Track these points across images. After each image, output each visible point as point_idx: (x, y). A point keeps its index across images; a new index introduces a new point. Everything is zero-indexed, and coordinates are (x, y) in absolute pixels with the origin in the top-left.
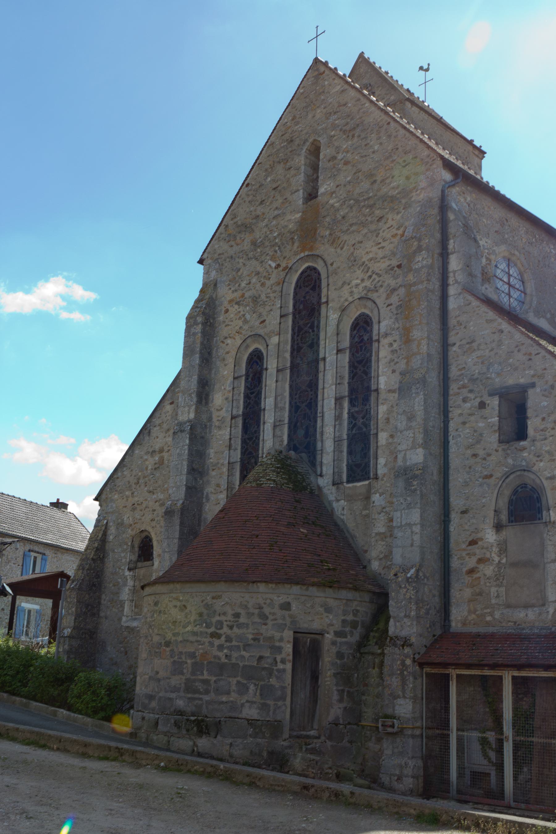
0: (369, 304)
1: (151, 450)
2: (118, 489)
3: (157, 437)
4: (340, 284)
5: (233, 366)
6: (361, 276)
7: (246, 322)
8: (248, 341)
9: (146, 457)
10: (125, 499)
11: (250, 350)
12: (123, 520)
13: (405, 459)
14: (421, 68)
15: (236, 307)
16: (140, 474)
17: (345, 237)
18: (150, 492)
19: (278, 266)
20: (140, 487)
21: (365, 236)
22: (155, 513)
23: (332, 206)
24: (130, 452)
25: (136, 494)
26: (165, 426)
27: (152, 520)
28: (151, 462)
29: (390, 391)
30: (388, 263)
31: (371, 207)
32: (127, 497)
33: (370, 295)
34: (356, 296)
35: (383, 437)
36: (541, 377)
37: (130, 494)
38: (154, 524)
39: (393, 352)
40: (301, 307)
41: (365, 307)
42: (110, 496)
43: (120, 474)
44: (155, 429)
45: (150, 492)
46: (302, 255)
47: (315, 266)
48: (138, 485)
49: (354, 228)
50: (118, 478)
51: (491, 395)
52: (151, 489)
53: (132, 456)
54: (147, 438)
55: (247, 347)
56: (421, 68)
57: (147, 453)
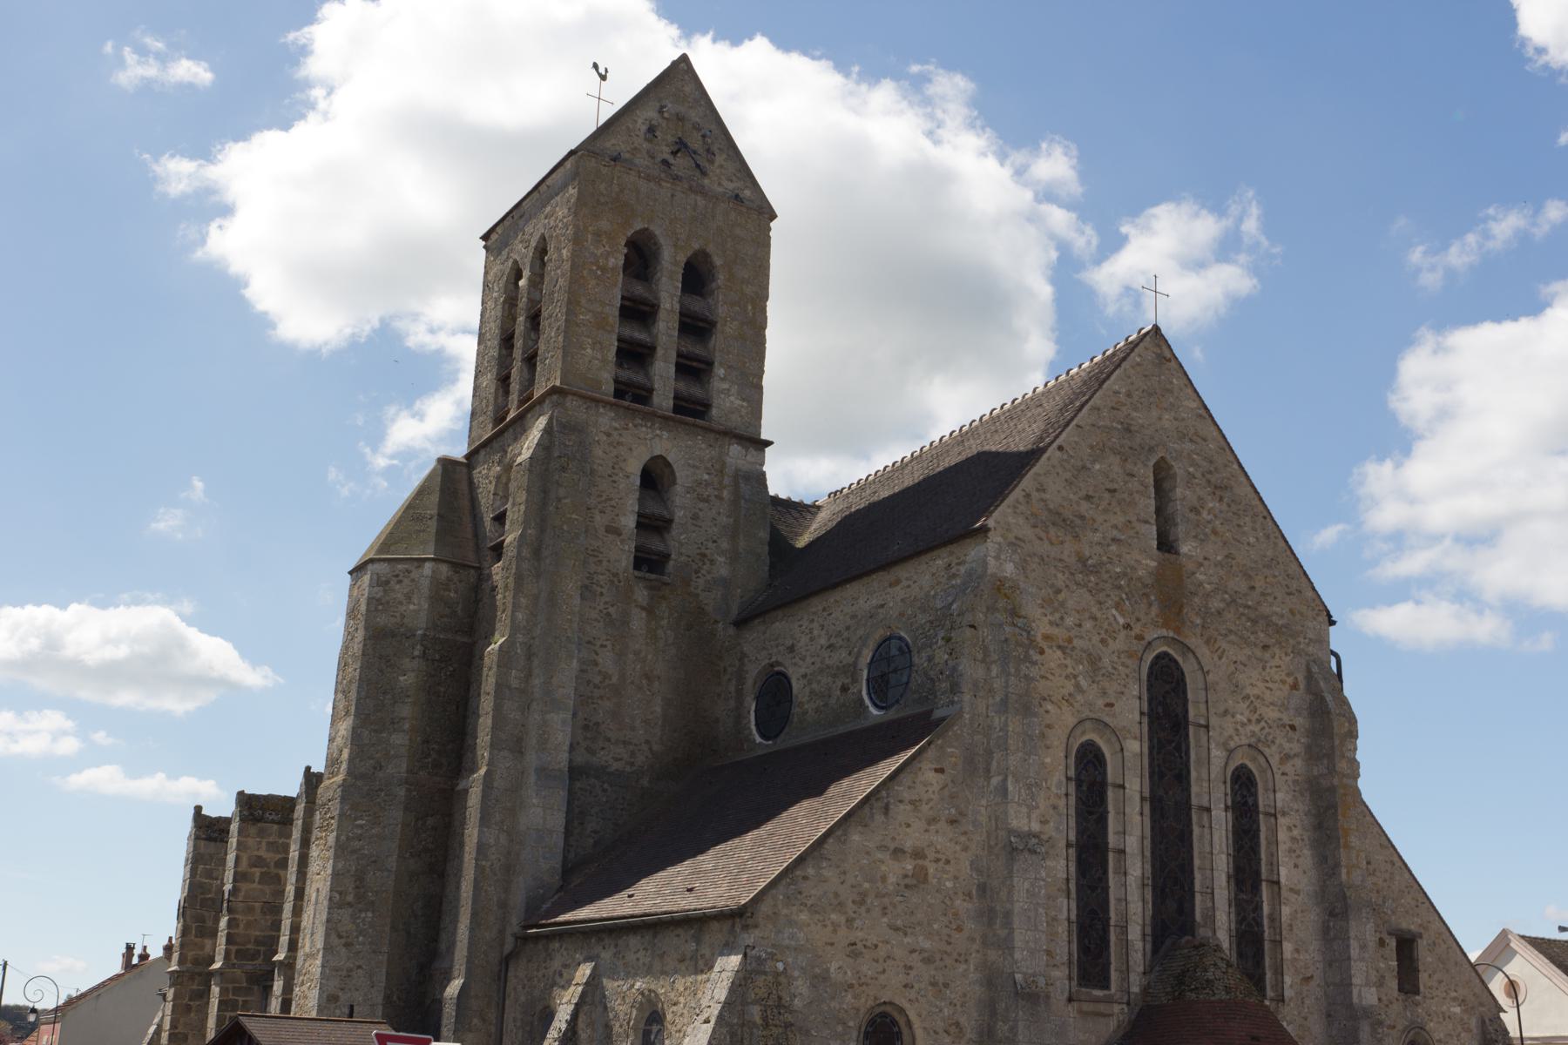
0: (1262, 760)
1: (892, 846)
2: (809, 903)
3: (909, 826)
4: (1222, 709)
5: (1062, 755)
6: (1247, 713)
7: (1078, 686)
8: (1088, 725)
9: (879, 855)
10: (830, 928)
11: (1084, 739)
12: (827, 970)
13: (1360, 995)
14: (595, 66)
15: (1059, 653)
16: (866, 885)
17: (1224, 645)
18: (897, 929)
19: (1127, 627)
20: (868, 911)
21: (1249, 657)
22: (913, 973)
23: (1201, 584)
24: (839, 833)
25: (858, 923)
26: (925, 808)
27: (905, 986)
28: (894, 871)
29: (1291, 890)
30: (1276, 715)
31: (1254, 622)
32: (836, 926)
33: (1260, 746)
34: (1245, 741)
35: (1288, 947)
36: (1426, 929)
37: (843, 919)
38: (912, 994)
39: (1293, 839)
40: (1160, 709)
41: (1254, 759)
42: (785, 911)
43: (811, 871)
44: (902, 807)
45: (897, 929)
46: (1164, 632)
47: (1180, 660)
48: (863, 909)
49: (1232, 637)
50: (805, 878)
51: (1390, 934)
52: (899, 923)
53: (844, 843)
54: (879, 818)
55: (1083, 733)
56: (595, 66)
57: (882, 848)
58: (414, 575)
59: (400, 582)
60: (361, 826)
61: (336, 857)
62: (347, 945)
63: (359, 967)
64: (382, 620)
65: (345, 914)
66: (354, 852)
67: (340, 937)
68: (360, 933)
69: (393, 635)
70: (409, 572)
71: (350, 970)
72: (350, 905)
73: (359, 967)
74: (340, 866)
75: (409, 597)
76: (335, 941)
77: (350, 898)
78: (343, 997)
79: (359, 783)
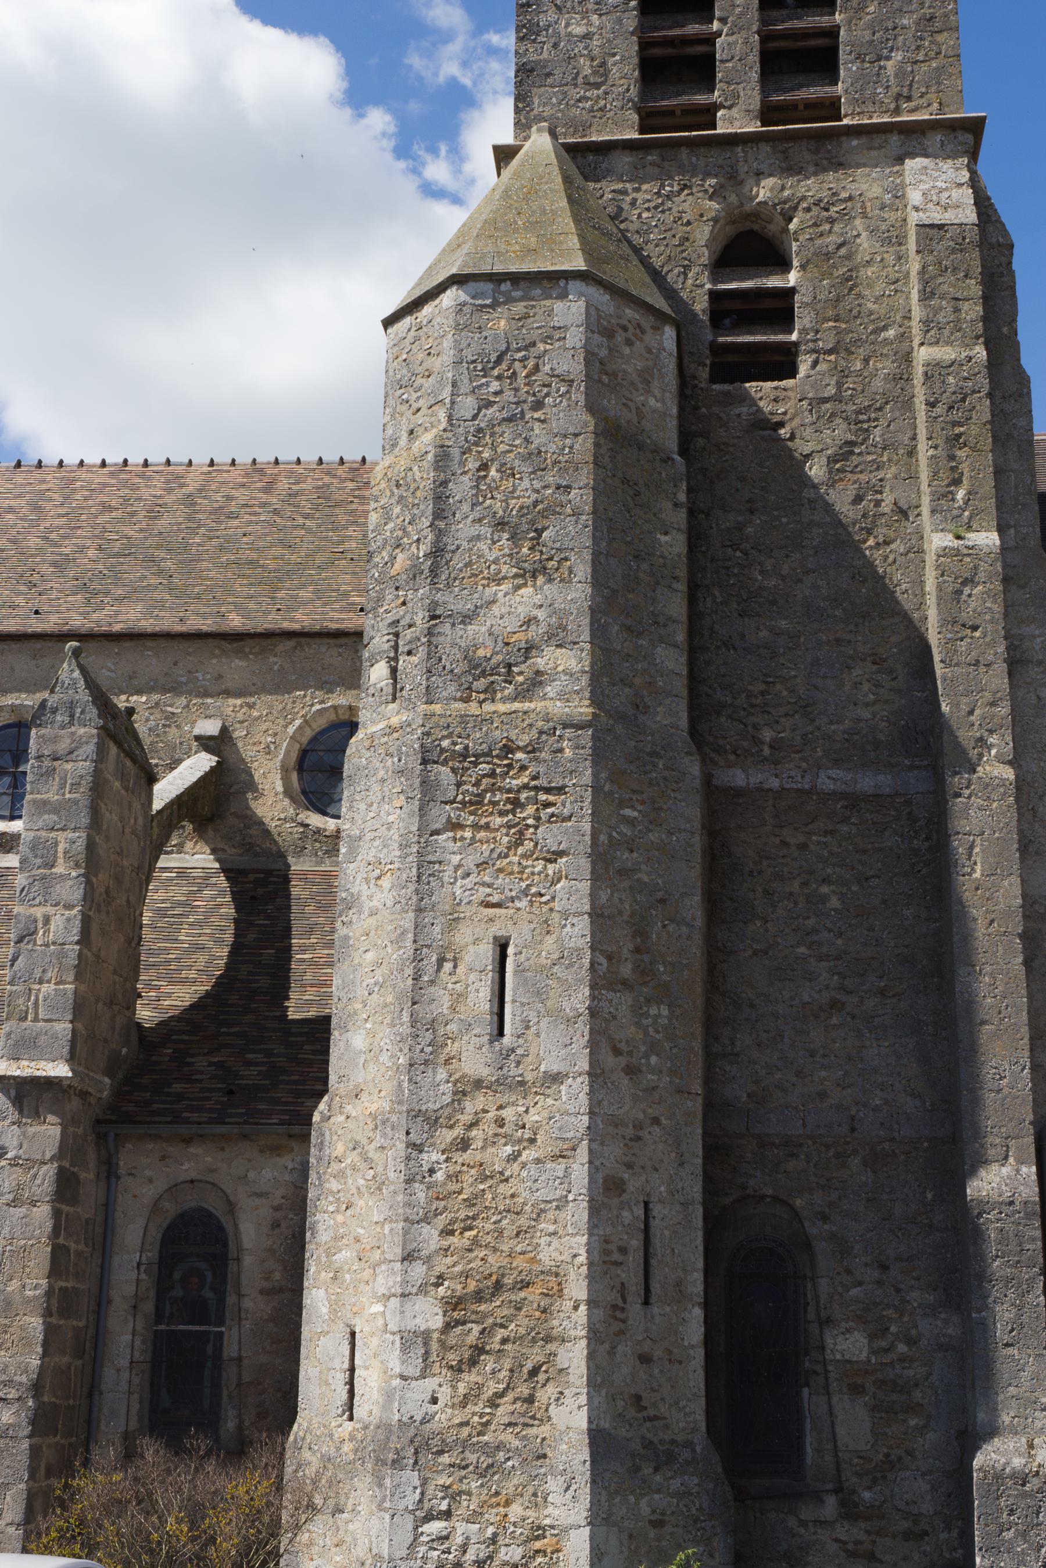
58: (649, 338)
59: (629, 343)
60: (631, 822)
61: (595, 878)
62: (631, 1071)
63: (656, 1121)
64: (611, 404)
65: (622, 1002)
66: (621, 872)
67: (617, 1052)
68: (654, 1048)
69: (641, 447)
70: (643, 332)
71: (638, 1126)
72: (624, 982)
73: (656, 1121)
74: (604, 896)
75: (646, 377)
76: (610, 1060)
77: (626, 970)
78: (633, 1184)
79: (619, 729)
